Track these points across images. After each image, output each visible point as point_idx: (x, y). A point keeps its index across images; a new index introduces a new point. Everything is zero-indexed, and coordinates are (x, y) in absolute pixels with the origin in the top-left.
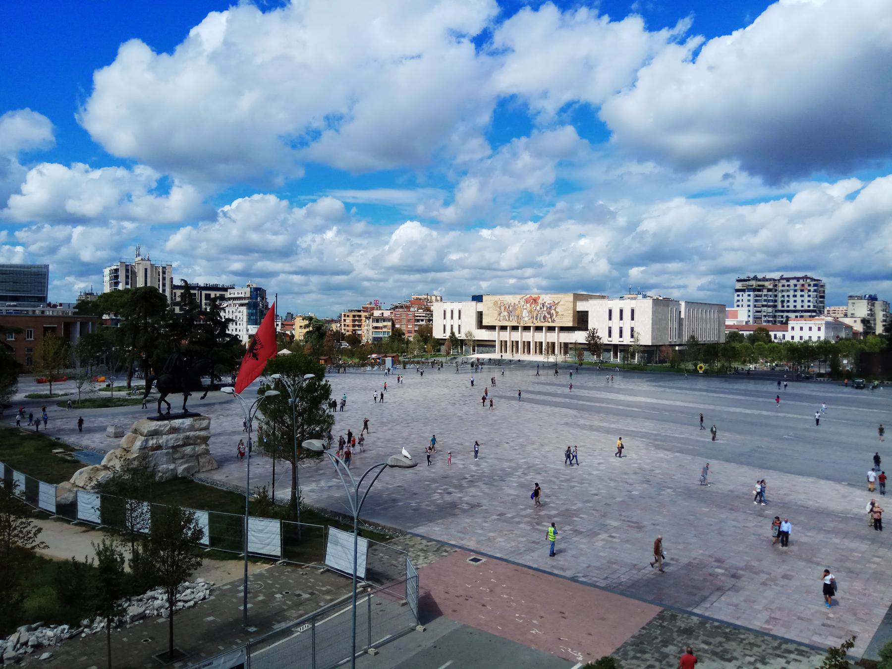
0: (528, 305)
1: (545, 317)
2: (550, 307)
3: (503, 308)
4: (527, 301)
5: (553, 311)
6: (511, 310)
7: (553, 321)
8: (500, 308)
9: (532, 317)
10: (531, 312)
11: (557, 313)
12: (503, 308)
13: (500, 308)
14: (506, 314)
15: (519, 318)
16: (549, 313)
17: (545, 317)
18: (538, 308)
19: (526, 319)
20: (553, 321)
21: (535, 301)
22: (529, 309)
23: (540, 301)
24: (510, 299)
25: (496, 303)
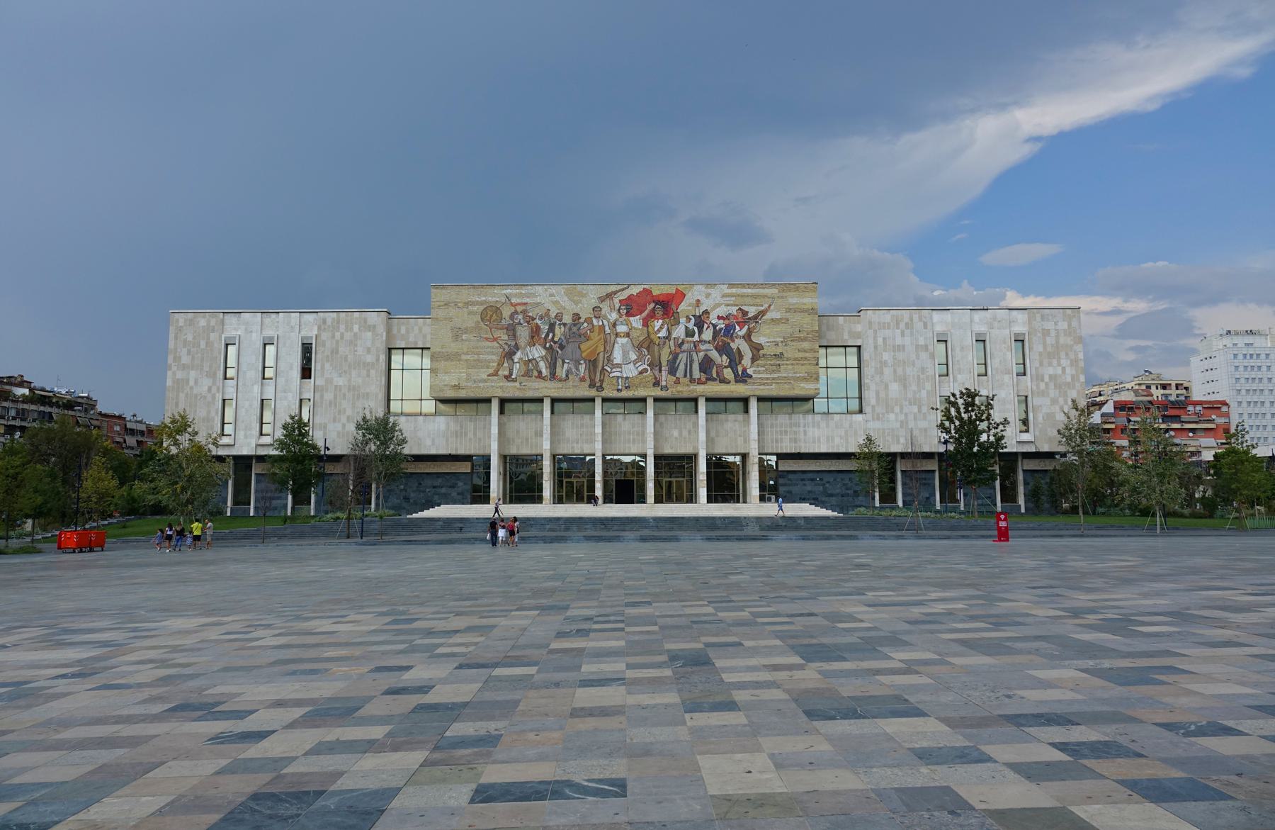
0: (636, 322)
1: (706, 365)
2: (729, 330)
3: (523, 333)
4: (631, 307)
5: (739, 344)
6: (567, 341)
7: (743, 378)
8: (511, 330)
9: (655, 365)
10: (646, 345)
11: (756, 348)
12: (523, 333)
13: (511, 330)
14: (538, 352)
15: (596, 368)
16: (724, 349)
17: (706, 365)
18: (679, 332)
19: (630, 371)
20: (743, 378)
21: (666, 306)
22: (639, 335)
23: (682, 307)
24: (550, 298)
25: (490, 314)
